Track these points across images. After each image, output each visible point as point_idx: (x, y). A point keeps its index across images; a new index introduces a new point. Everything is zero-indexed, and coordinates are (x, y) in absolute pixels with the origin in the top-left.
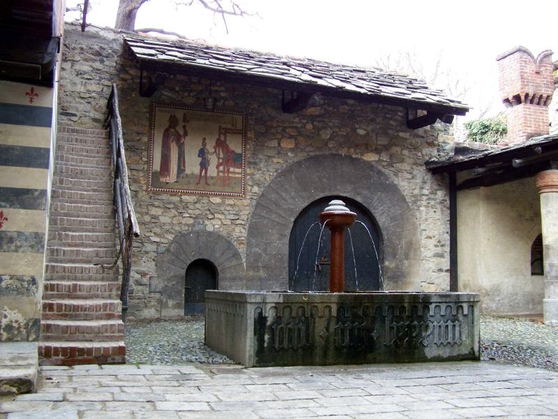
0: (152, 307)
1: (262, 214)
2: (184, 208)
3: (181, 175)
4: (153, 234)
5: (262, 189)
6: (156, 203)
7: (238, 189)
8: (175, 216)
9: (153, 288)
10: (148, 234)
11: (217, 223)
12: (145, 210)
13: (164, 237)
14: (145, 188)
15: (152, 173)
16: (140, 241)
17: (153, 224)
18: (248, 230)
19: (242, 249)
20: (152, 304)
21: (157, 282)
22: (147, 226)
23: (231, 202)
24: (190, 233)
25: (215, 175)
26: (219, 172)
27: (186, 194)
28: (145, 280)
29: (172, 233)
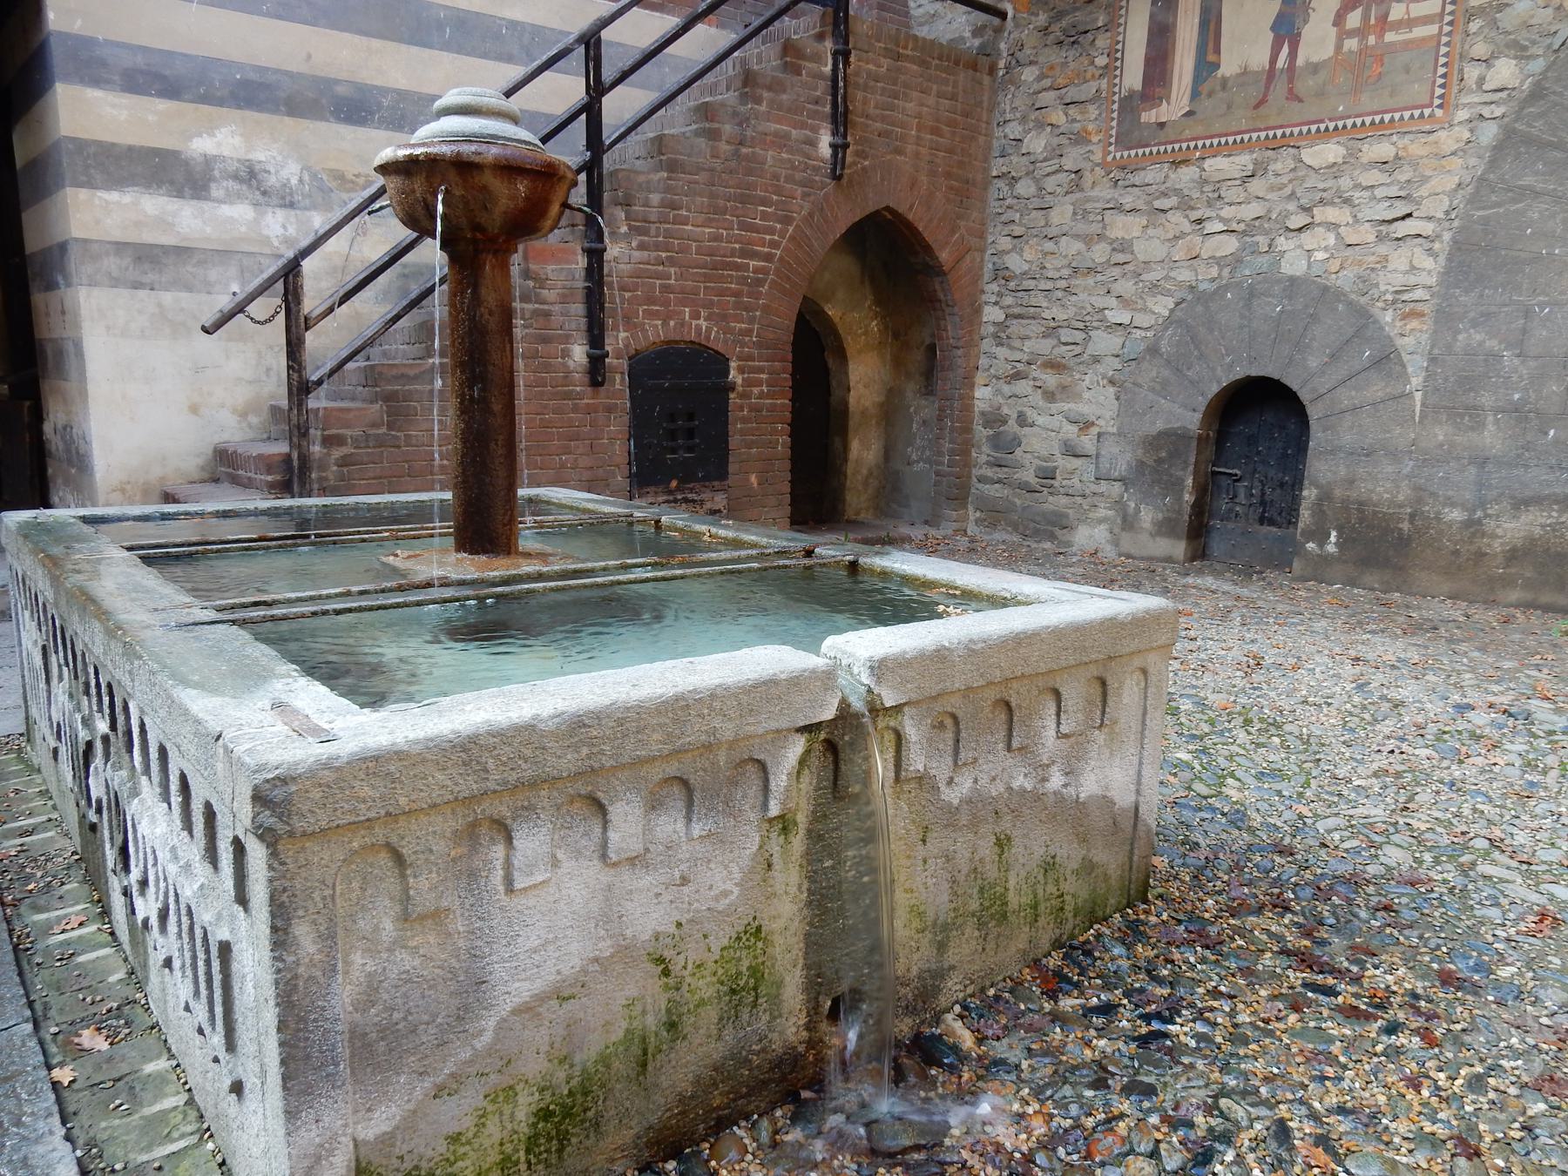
0: (1101, 521)
1: (1528, 180)
2: (1209, 204)
3: (1206, 88)
4: (1113, 302)
5: (1538, 65)
6: (1128, 200)
7: (1418, 91)
8: (1182, 235)
9: (1105, 464)
10: (1099, 302)
11: (1320, 242)
12: (1095, 228)
13: (1145, 310)
14: (1098, 157)
15: (1120, 99)
16: (1081, 325)
17: (1116, 271)
18: (1449, 259)
19: (1412, 340)
20: (1102, 512)
21: (1116, 450)
22: (1099, 277)
23: (1384, 150)
24: (1226, 288)
25: (1327, 52)
26: (1343, 34)
27: (1215, 152)
28: (1087, 443)
29: (1168, 294)
